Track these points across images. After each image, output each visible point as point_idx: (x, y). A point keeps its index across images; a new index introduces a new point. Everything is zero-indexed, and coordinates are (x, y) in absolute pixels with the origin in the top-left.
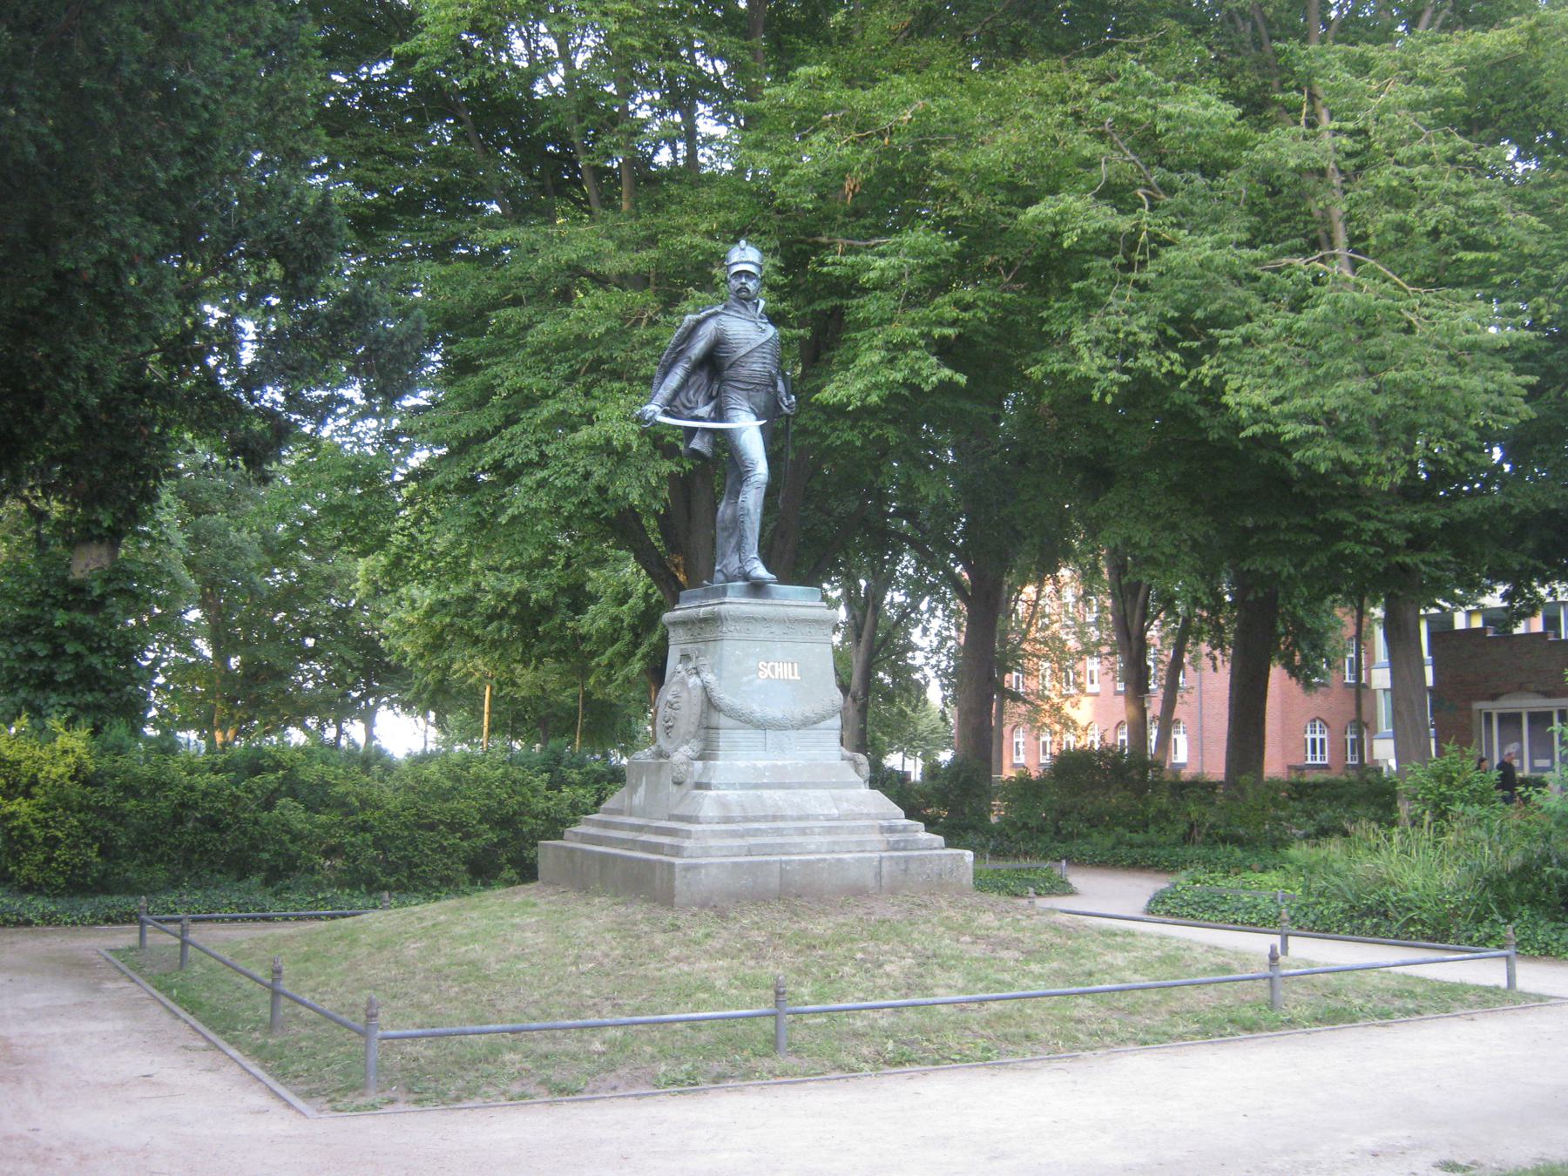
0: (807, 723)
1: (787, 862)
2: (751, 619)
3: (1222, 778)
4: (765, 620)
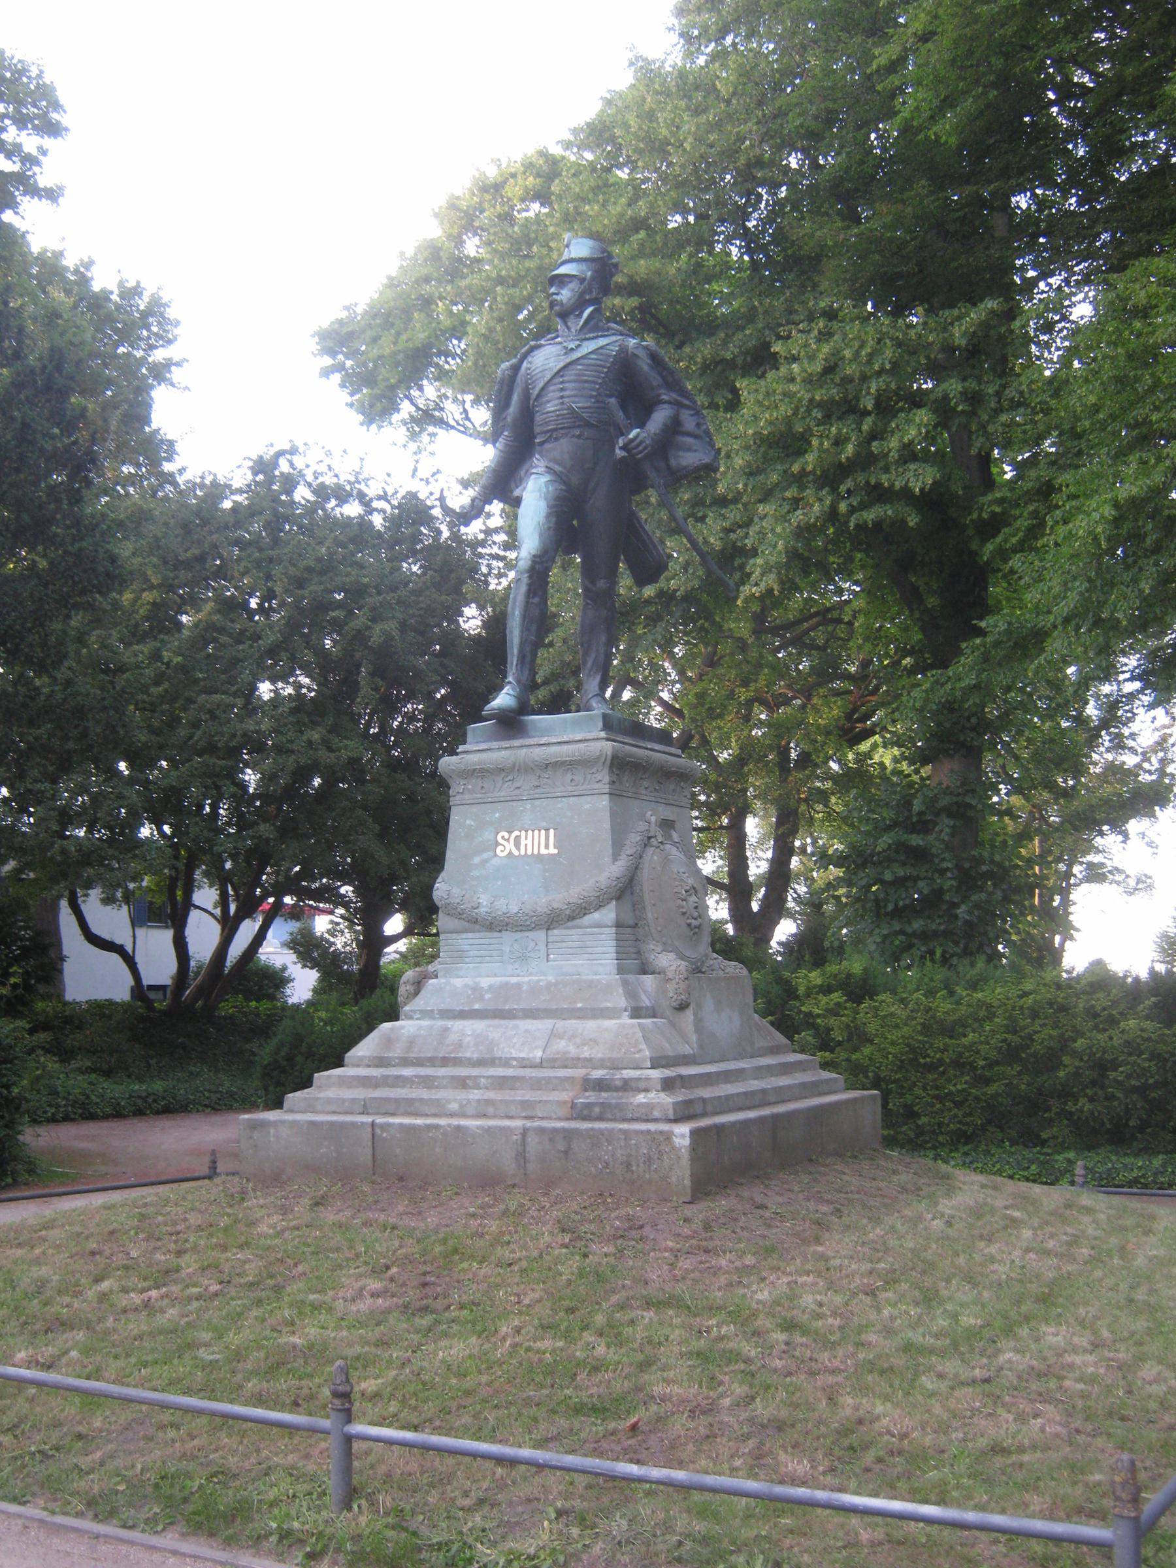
0: (553, 920)
1: (384, 1127)
2: (500, 771)
3: (69, 997)
4: (525, 769)
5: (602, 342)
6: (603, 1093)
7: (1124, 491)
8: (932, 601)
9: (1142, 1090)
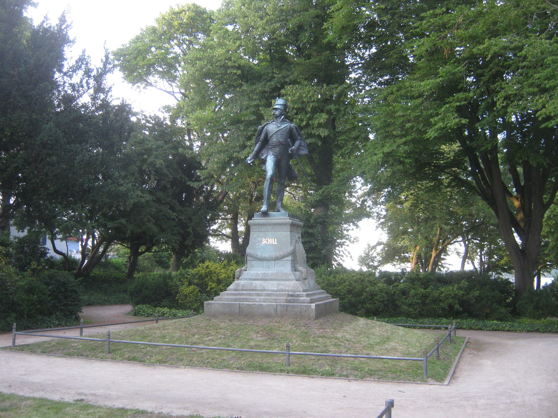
0: (277, 259)
1: (242, 304)
2: (263, 224)
5: (286, 125)
6: (292, 297)
7: (386, 149)
8: (317, 161)
9: (382, 302)
